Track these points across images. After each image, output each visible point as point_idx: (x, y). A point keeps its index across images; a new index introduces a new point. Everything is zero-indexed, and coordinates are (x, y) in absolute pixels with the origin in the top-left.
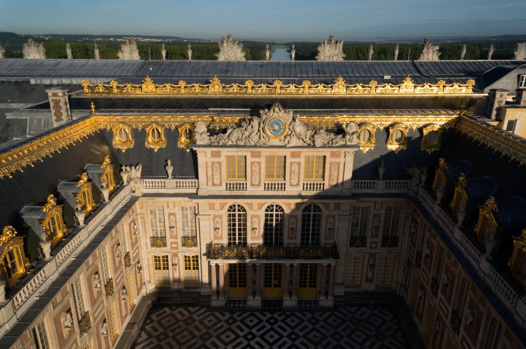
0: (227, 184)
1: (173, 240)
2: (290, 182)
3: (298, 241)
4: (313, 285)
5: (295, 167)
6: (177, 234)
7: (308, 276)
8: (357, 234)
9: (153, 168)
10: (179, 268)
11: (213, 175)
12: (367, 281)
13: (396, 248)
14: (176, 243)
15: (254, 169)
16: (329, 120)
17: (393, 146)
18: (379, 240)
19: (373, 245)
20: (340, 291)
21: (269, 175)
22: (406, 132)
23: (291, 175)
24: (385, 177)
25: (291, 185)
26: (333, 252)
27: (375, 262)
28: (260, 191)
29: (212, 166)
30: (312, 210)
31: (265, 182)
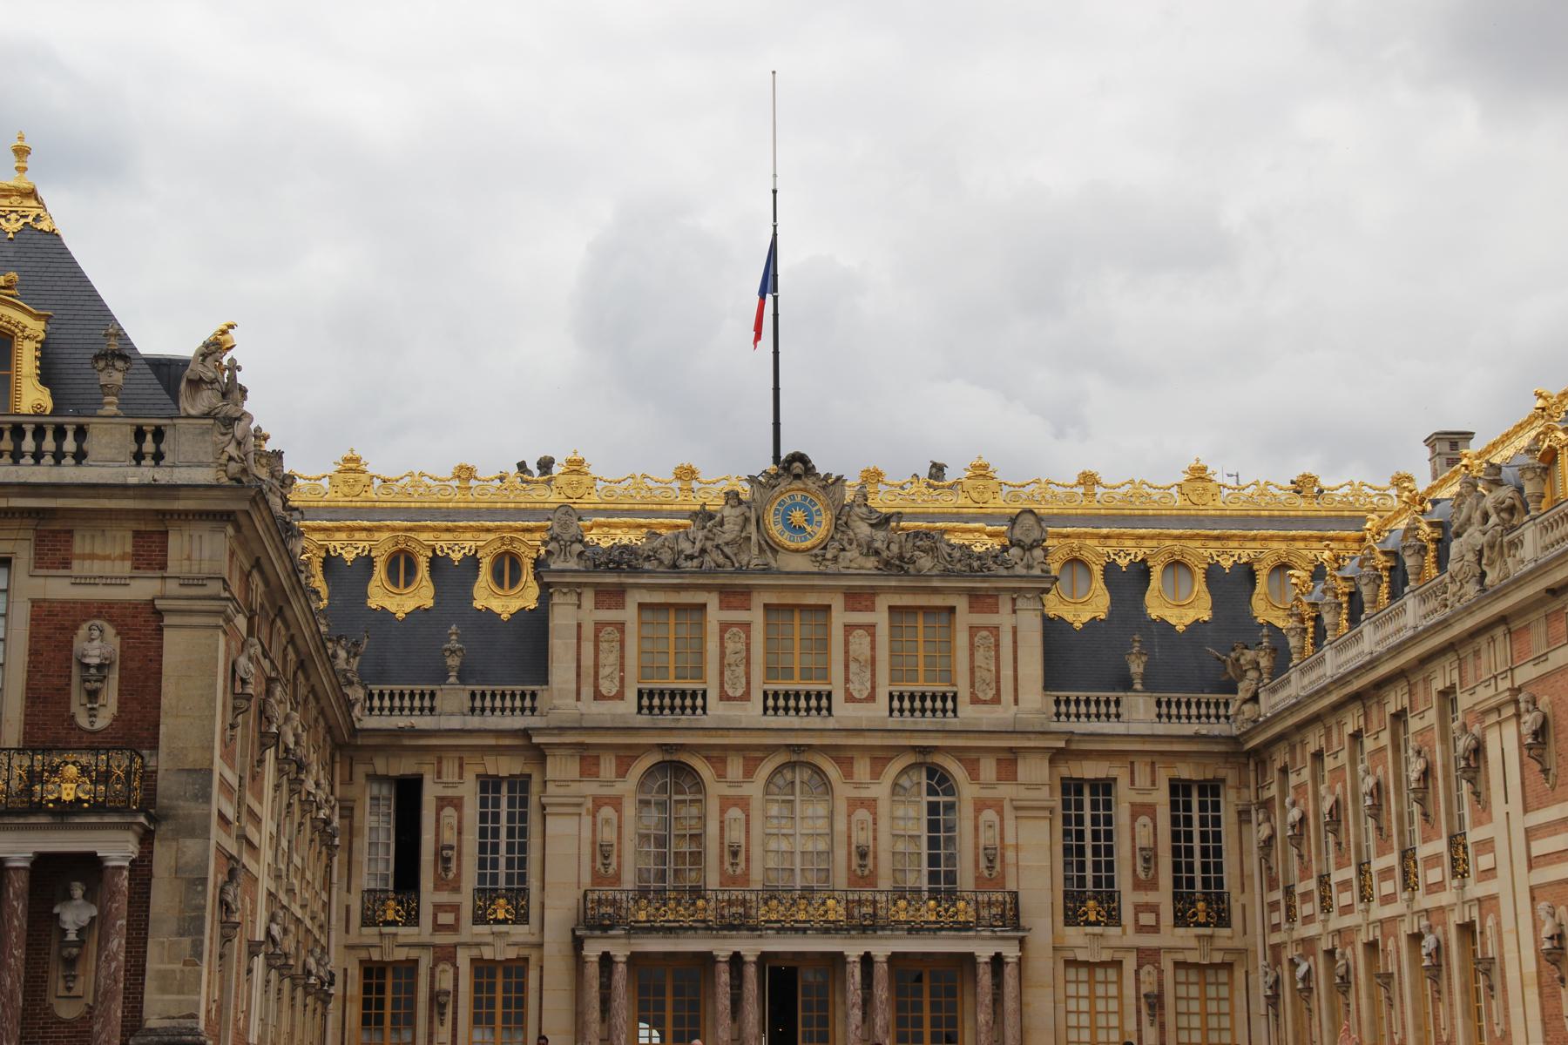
0: (640, 694)
1: (444, 897)
2: (847, 690)
5: (860, 644)
6: (458, 875)
10: (455, 1013)
11: (596, 666)
13: (1225, 932)
14: (455, 908)
15: (730, 646)
18: (1163, 897)
19: (1147, 919)
23: (847, 667)
25: (849, 698)
27: (1160, 985)
29: (596, 636)
31: (766, 687)
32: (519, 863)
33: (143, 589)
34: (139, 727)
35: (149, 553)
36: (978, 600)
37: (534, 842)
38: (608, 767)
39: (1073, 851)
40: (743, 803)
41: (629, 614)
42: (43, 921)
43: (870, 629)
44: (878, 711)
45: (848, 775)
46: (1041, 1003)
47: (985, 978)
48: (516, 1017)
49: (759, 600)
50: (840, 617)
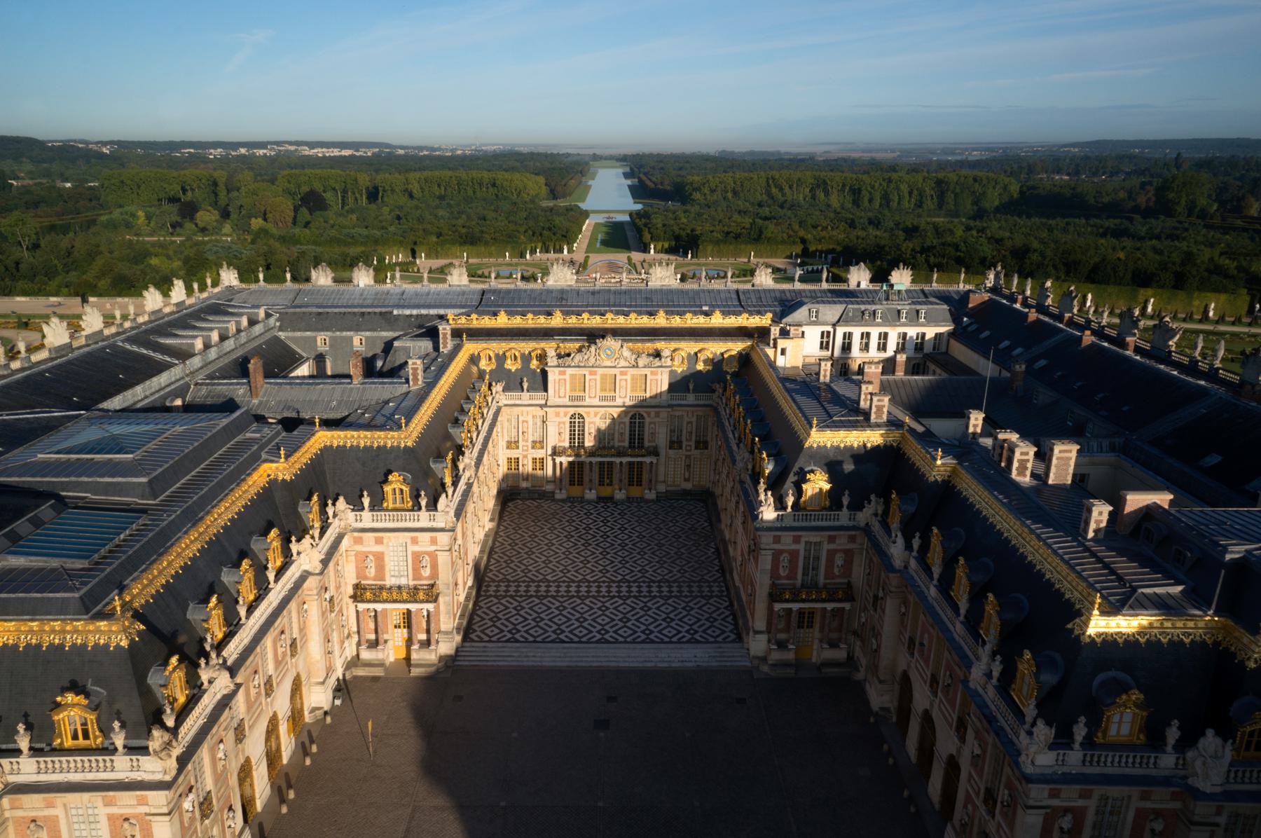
3: (626, 444)
4: (640, 484)
5: (623, 383)
7: (635, 475)
8: (675, 439)
9: (514, 383)
12: (686, 480)
16: (650, 346)
17: (700, 366)
20: (662, 488)
21: (603, 390)
22: (711, 356)
24: (694, 391)
26: (655, 452)
28: (596, 402)
30: (636, 416)
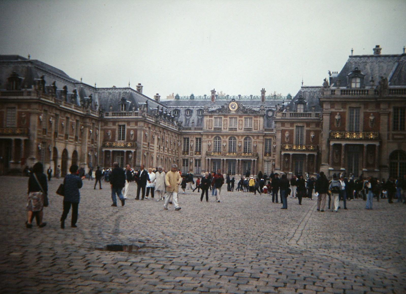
1: (191, 152)
15: (225, 123)
25: (239, 129)
32: (200, 148)
33: (136, 127)
34: (135, 140)
35: (136, 124)
36: (256, 117)
37: (202, 145)
38: (210, 137)
39: (266, 148)
40: (226, 141)
41: (213, 118)
42: (127, 157)
43: (242, 120)
44: (242, 131)
45: (238, 138)
46: (260, 165)
47: (253, 162)
48: (199, 166)
49: (228, 117)
50: (238, 119)
